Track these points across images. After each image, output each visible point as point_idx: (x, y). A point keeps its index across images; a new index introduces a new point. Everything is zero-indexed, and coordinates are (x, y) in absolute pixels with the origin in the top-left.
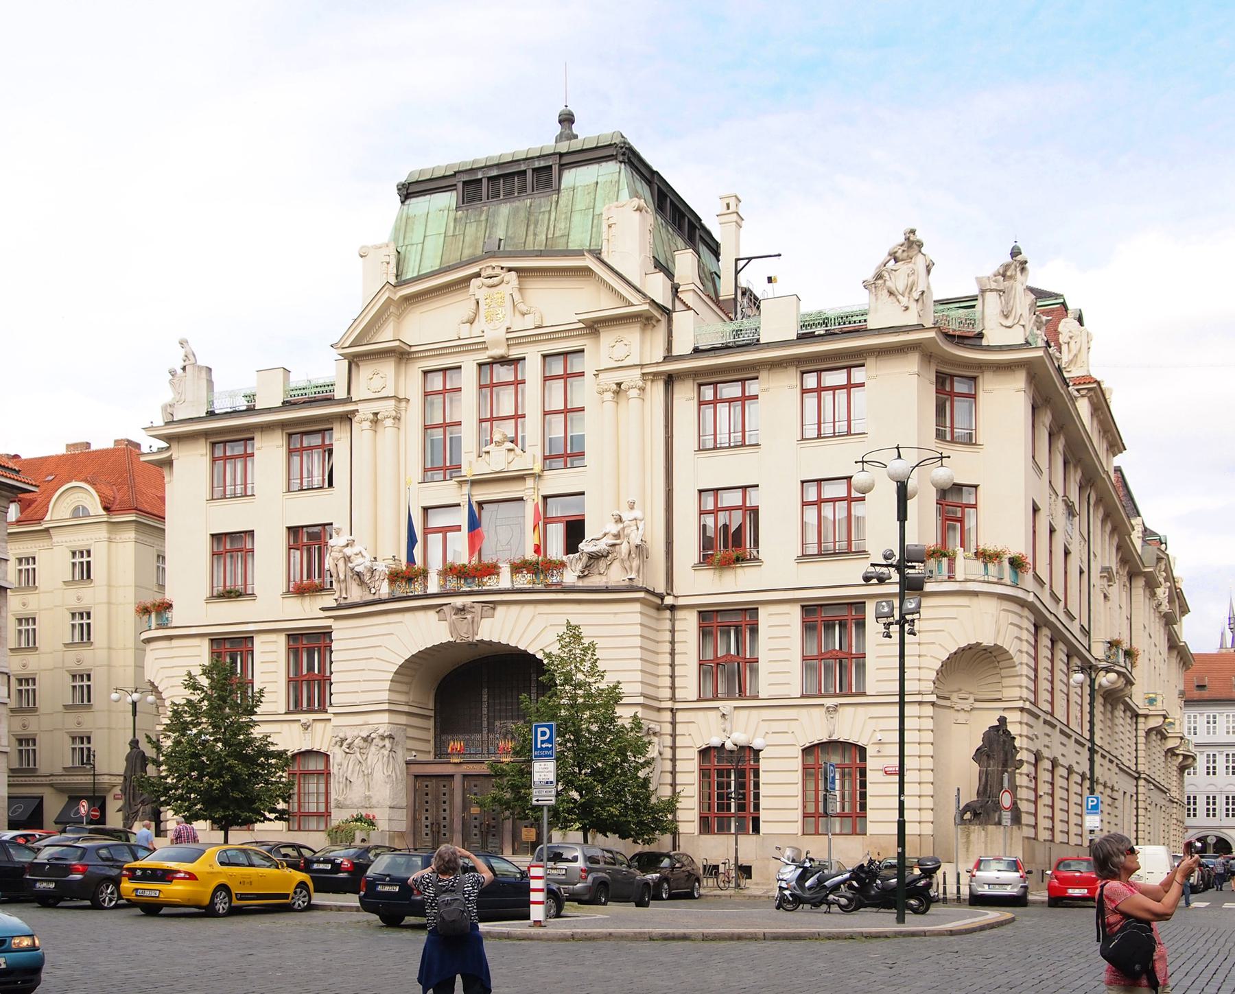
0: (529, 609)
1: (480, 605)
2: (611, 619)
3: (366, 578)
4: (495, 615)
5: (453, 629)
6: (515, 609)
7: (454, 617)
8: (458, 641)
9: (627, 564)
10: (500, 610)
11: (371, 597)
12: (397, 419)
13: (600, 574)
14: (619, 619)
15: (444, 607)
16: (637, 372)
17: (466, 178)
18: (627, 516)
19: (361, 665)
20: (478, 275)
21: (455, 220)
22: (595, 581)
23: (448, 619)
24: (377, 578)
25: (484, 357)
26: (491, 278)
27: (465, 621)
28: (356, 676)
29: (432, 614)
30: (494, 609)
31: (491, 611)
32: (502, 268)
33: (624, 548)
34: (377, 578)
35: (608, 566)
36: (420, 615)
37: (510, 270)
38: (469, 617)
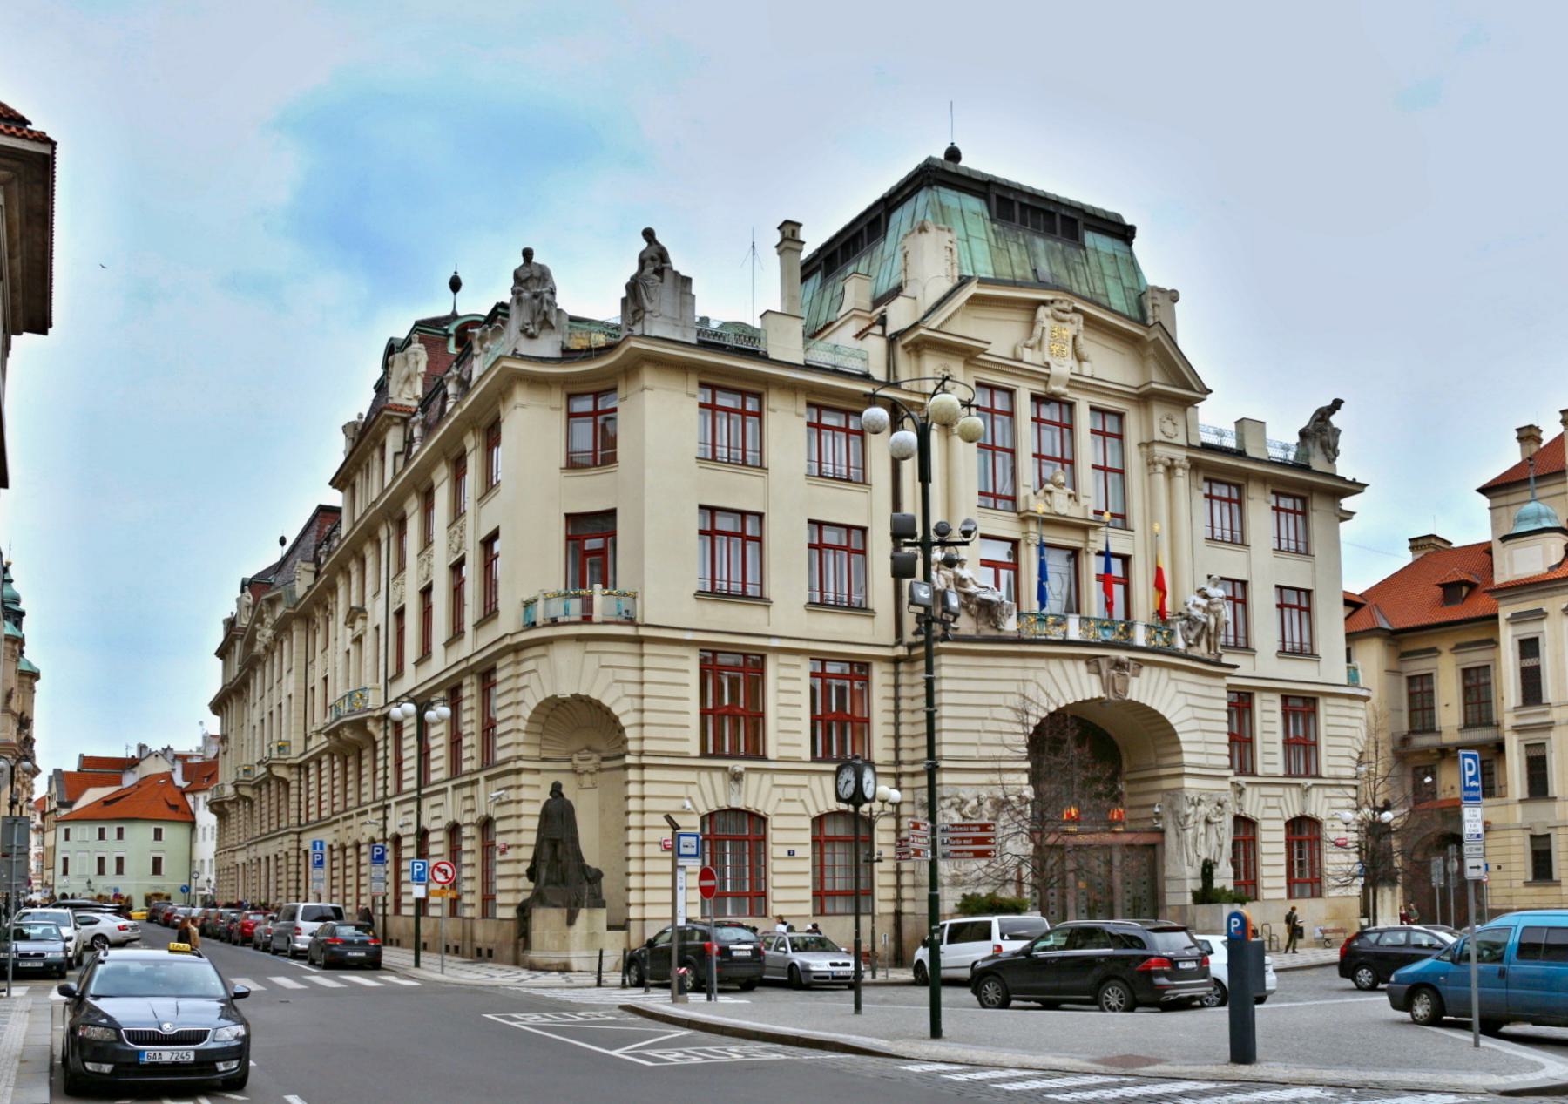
0: (1164, 672)
2: (1205, 691)
5: (1107, 684)
6: (1156, 671)
7: (1114, 672)
8: (1112, 697)
9: (1212, 639)
10: (1145, 671)
11: (994, 633)
15: (1100, 660)
18: (1211, 591)
19: (984, 712)
22: (1194, 652)
23: (1104, 673)
28: (976, 725)
29: (1082, 665)
30: (1141, 667)
33: (1212, 621)
36: (1069, 664)
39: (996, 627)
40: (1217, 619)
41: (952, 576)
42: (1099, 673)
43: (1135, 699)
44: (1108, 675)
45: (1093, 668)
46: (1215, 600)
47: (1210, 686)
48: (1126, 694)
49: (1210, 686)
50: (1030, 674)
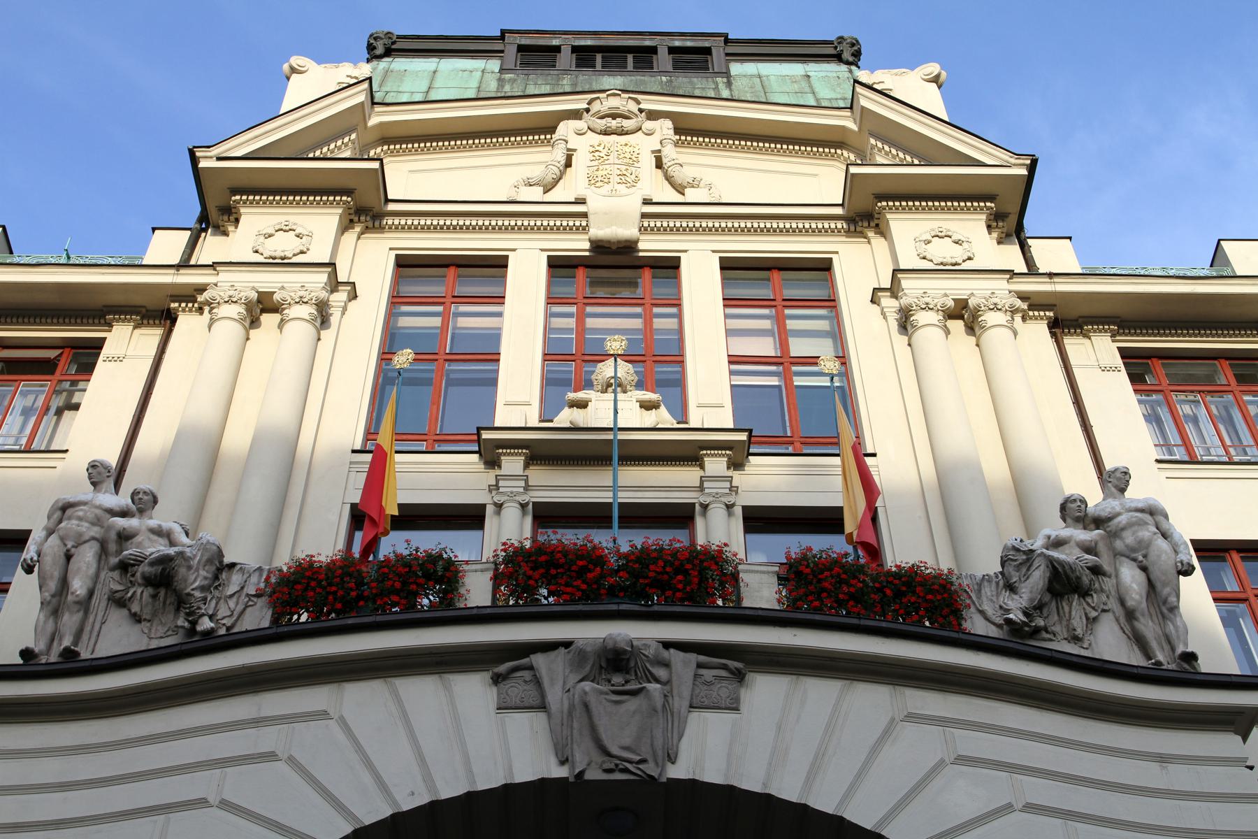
1: (693, 658)
3: (194, 580)
4: (744, 707)
7: (587, 686)
8: (592, 775)
9: (1148, 627)
12: (323, 317)
13: (1076, 639)
14: (1180, 777)
15: (538, 660)
16: (1001, 286)
17: (525, 41)
20: (576, 115)
21: (500, 80)
23: (555, 696)
24: (232, 589)
25: (578, 245)
26: (614, 116)
27: (632, 704)
30: (739, 676)
31: (731, 685)
32: (641, 111)
34: (232, 589)
35: (1091, 621)
37: (653, 115)
38: (653, 687)
39: (192, 631)
40: (1144, 569)
41: (95, 531)
42: (542, 707)
43: (713, 775)
44: (572, 708)
45: (518, 688)
46: (1123, 519)
47: (1162, 759)
48: (672, 759)
49: (1162, 759)
50: (266, 739)
